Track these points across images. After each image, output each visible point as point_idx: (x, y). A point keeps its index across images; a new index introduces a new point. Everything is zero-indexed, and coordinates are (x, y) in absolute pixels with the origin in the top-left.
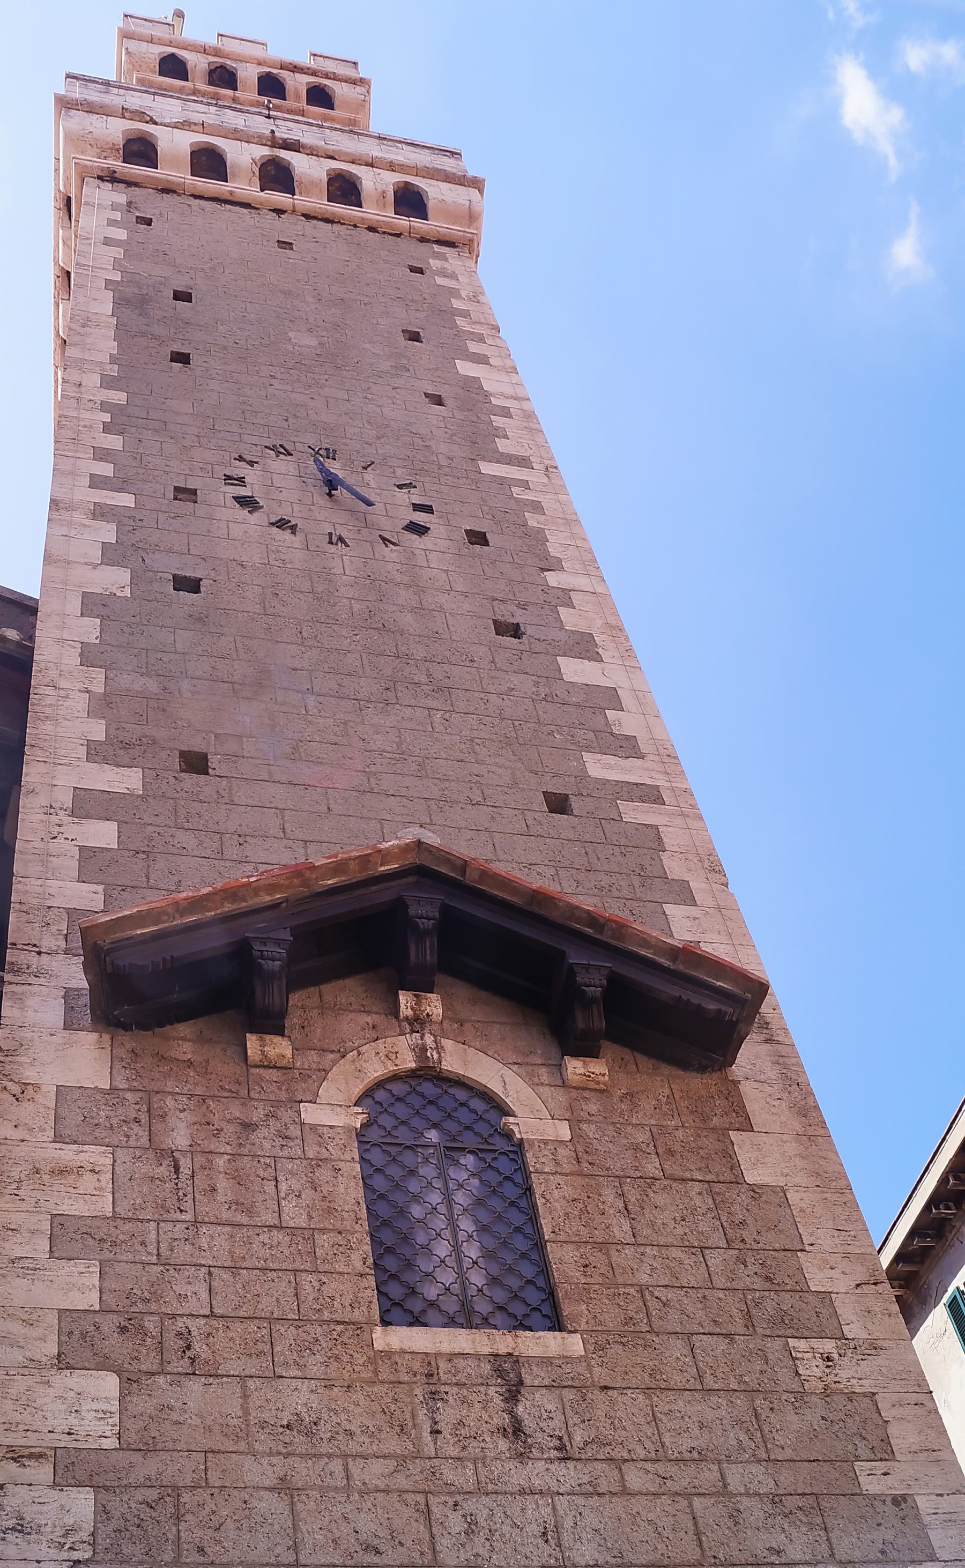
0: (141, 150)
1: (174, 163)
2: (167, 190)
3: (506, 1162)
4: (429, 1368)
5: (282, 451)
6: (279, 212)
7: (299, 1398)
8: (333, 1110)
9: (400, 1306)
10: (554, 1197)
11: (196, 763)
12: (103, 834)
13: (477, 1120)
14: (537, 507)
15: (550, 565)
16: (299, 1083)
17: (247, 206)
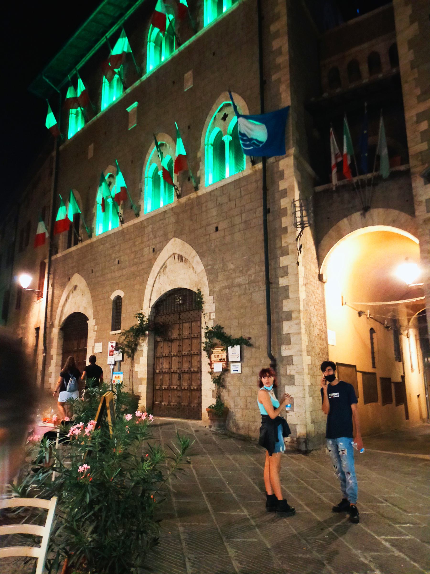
12: (424, 126)
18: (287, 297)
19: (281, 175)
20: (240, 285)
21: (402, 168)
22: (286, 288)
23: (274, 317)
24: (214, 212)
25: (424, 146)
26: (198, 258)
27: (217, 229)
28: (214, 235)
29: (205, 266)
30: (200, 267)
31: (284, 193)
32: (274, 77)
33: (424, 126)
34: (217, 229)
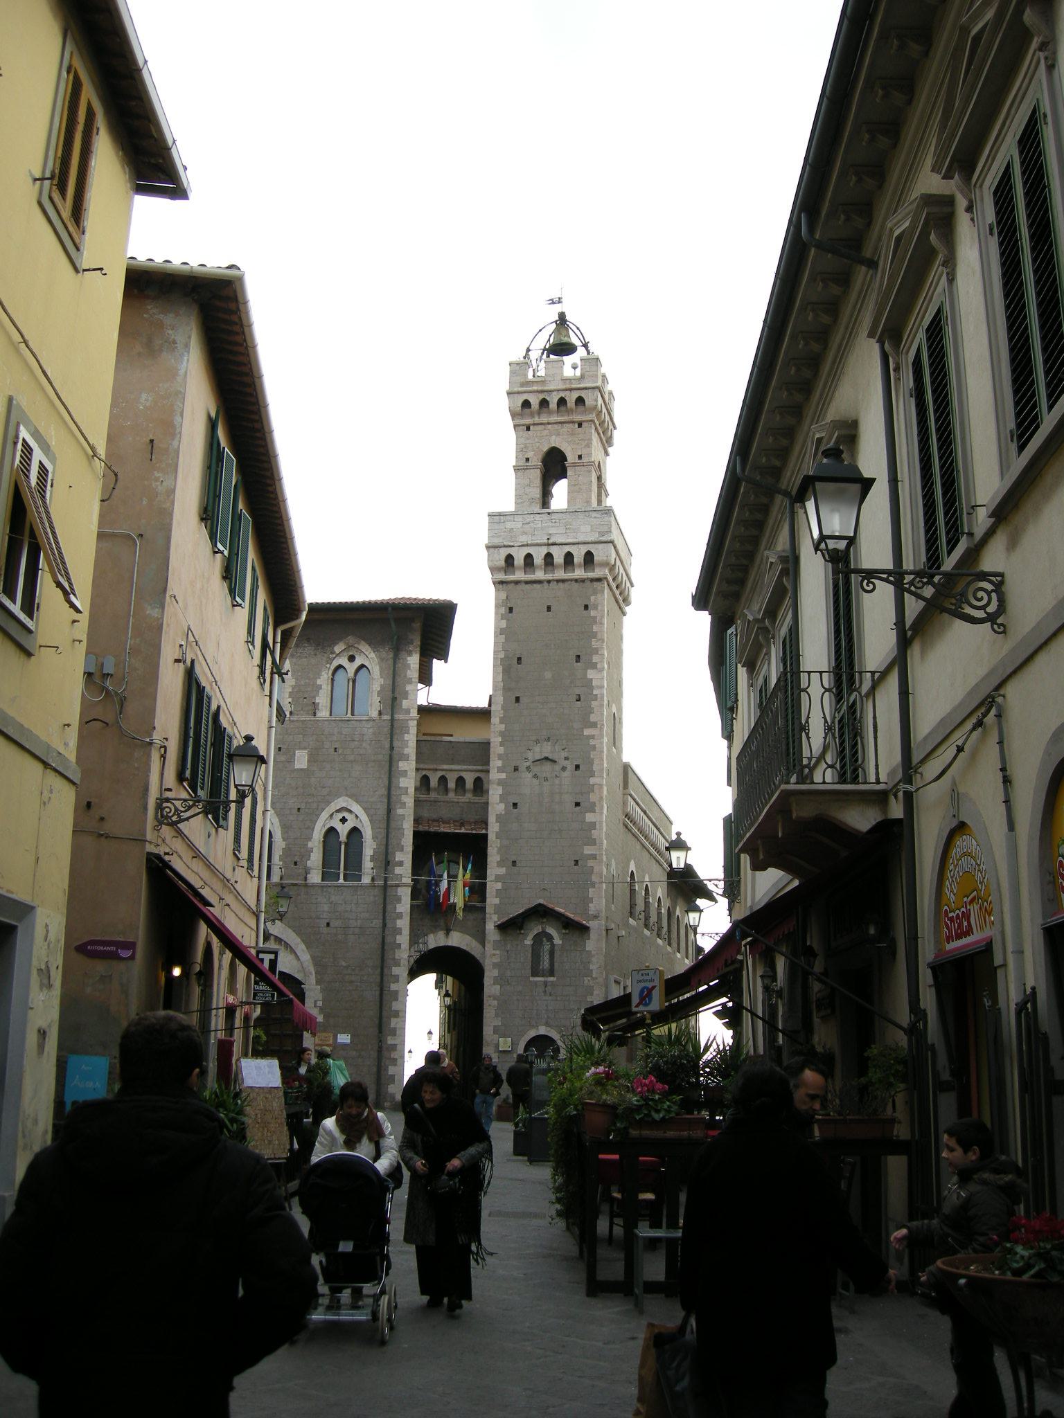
0: (509, 559)
1: (519, 568)
2: (517, 582)
3: (553, 945)
4: (536, 982)
5: (537, 741)
6: (549, 582)
7: (520, 988)
8: (529, 942)
9: (534, 974)
10: (557, 954)
11: (514, 863)
13: (550, 938)
14: (594, 748)
15: (592, 775)
16: (526, 935)
17: (540, 582)
18: (397, 999)
19: (399, 900)
20: (352, 982)
21: (478, 904)
22: (396, 992)
23: (384, 1013)
24: (326, 908)
25: (497, 901)
26: (303, 946)
27: (328, 924)
28: (325, 930)
29: (313, 958)
30: (305, 957)
31: (400, 916)
32: (400, 811)
33: (499, 886)
34: (328, 924)
